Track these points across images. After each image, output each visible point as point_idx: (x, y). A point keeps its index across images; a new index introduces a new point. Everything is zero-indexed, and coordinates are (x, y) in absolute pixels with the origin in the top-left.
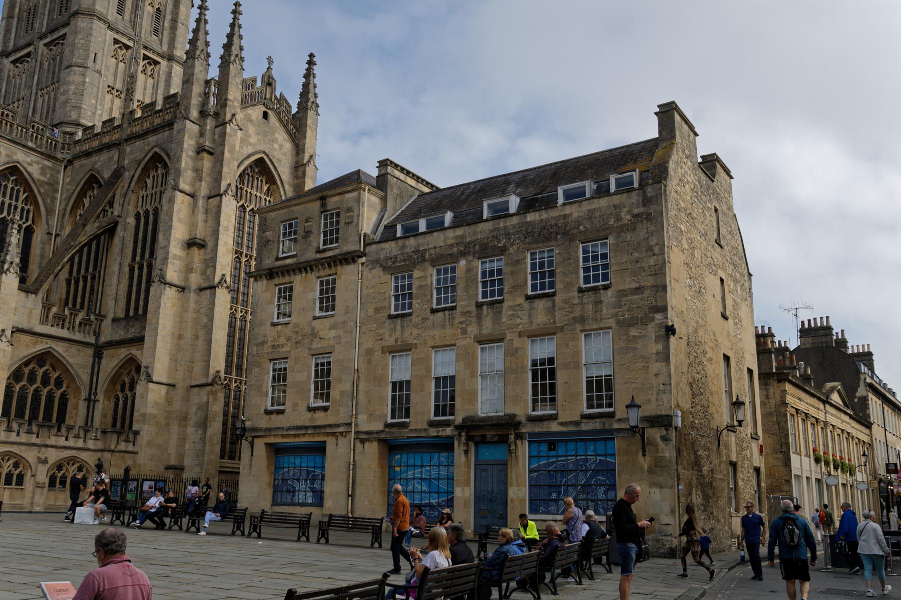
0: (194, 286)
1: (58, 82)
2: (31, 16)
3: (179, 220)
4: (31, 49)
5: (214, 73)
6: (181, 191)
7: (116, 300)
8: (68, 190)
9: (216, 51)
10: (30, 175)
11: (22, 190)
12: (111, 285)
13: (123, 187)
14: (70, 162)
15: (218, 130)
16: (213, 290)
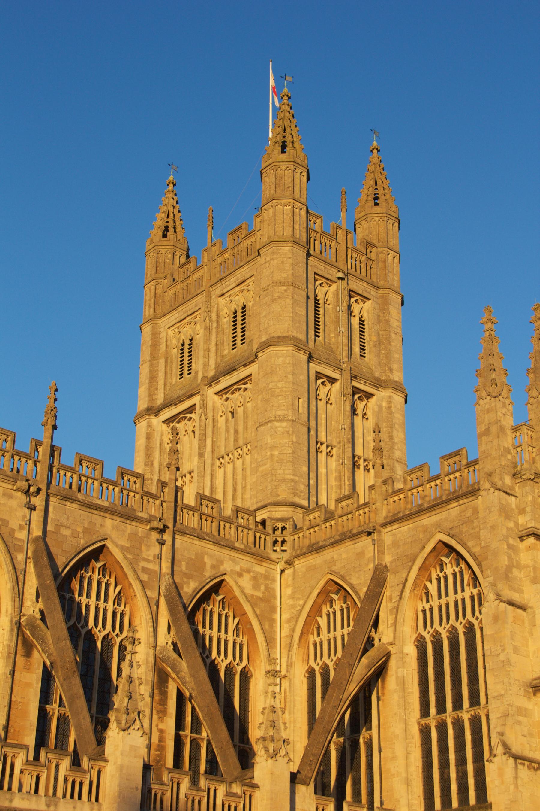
1: (246, 445)
2: (186, 354)
3: (516, 650)
4: (196, 400)
6: (511, 603)
7: (408, 782)
8: (293, 607)
10: (242, 591)
11: (231, 614)
12: (394, 758)
13: (391, 598)
14: (289, 563)
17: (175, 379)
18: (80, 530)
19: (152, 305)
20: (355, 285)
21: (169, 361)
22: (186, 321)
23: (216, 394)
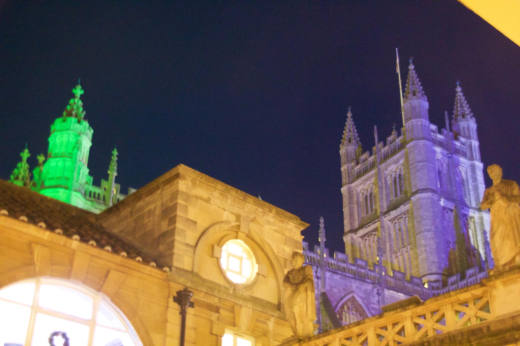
4: (378, 224)
17: (363, 215)
18: (341, 289)
19: (347, 178)
21: (359, 206)
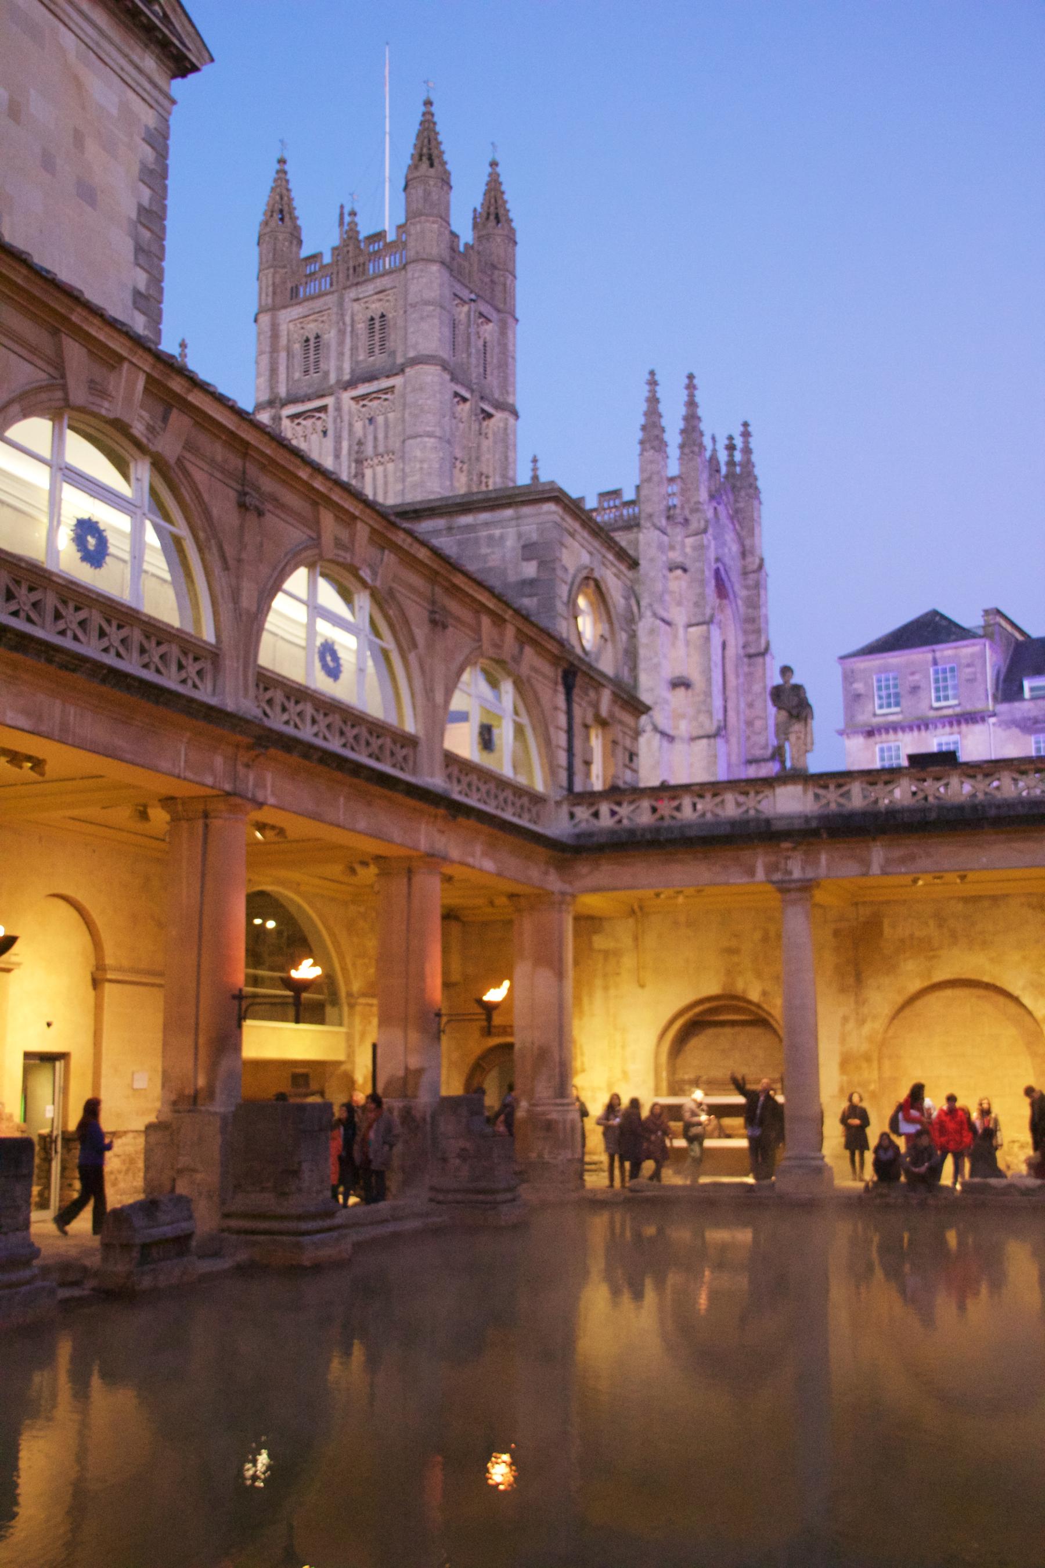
0: (686, 735)
2: (312, 352)
4: (329, 401)
5: (673, 469)
6: (663, 620)
9: (673, 438)
15: (689, 541)
16: (712, 740)
17: (297, 375)
19: (270, 294)
20: (485, 308)
22: (311, 318)
23: (353, 398)
